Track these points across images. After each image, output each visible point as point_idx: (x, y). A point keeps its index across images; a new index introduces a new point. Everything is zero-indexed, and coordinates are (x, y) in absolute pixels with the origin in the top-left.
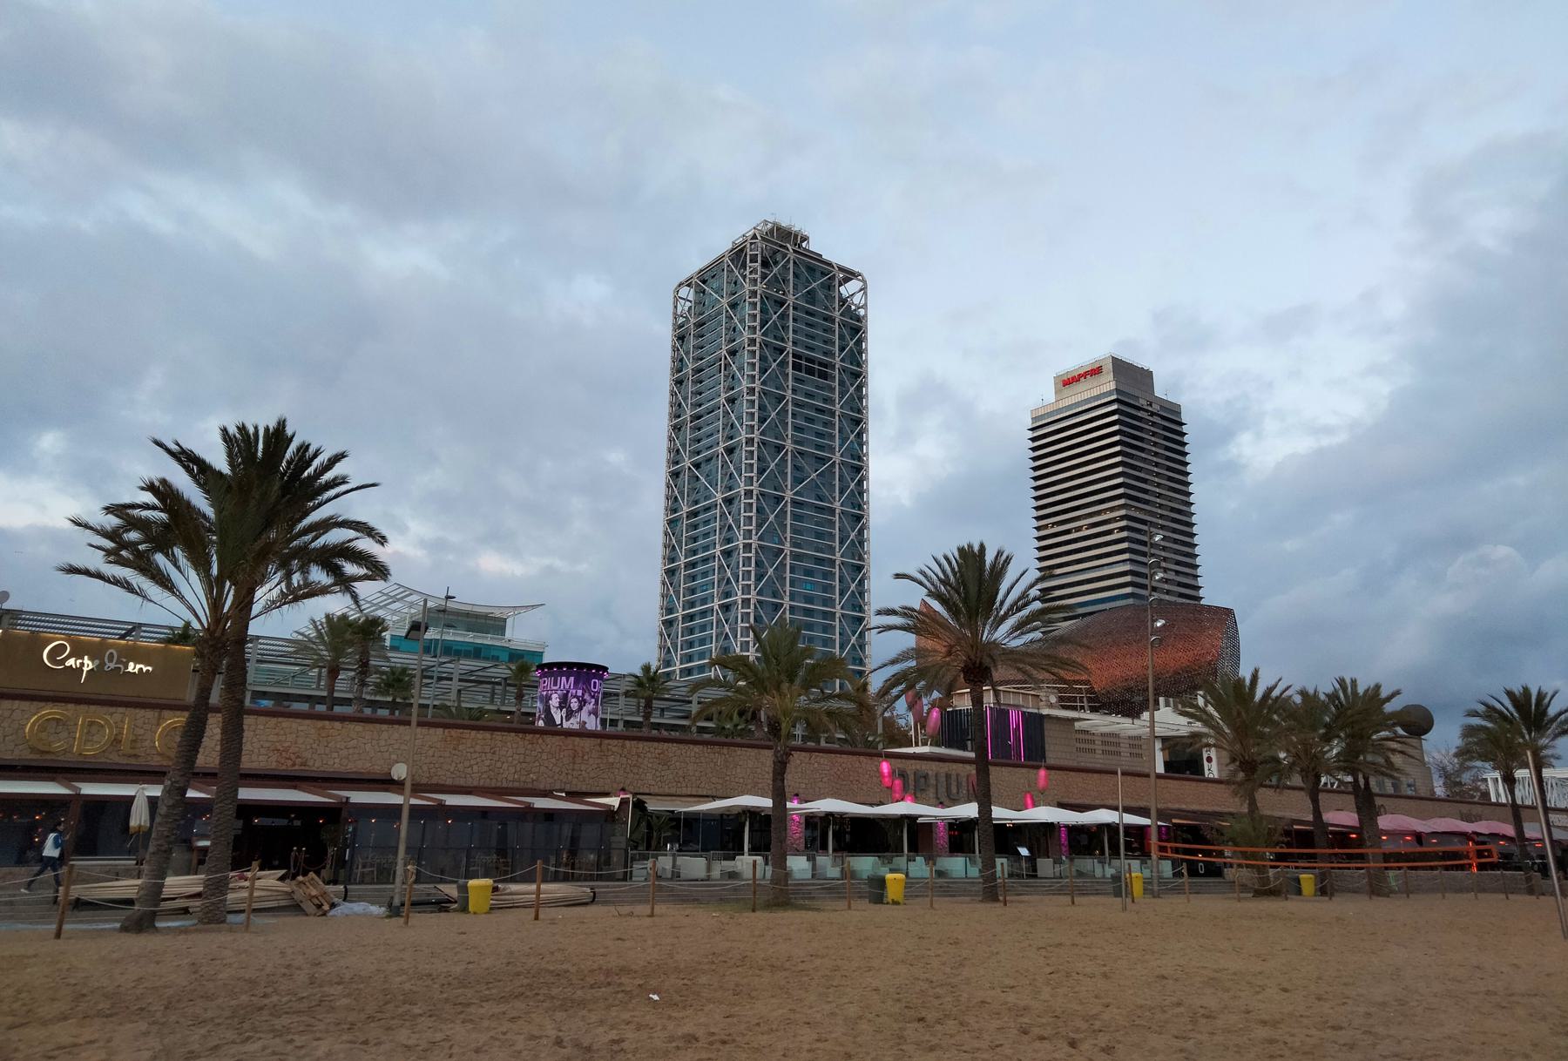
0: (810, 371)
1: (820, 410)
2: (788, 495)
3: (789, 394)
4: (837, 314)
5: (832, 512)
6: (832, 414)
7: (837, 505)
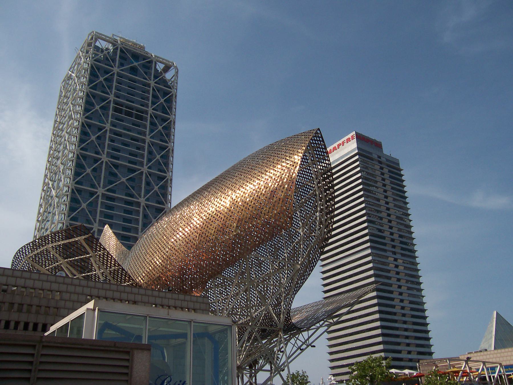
0: (129, 114)
1: (133, 139)
2: (100, 191)
3: (108, 126)
4: (152, 83)
5: (138, 204)
6: (144, 141)
7: (142, 201)
